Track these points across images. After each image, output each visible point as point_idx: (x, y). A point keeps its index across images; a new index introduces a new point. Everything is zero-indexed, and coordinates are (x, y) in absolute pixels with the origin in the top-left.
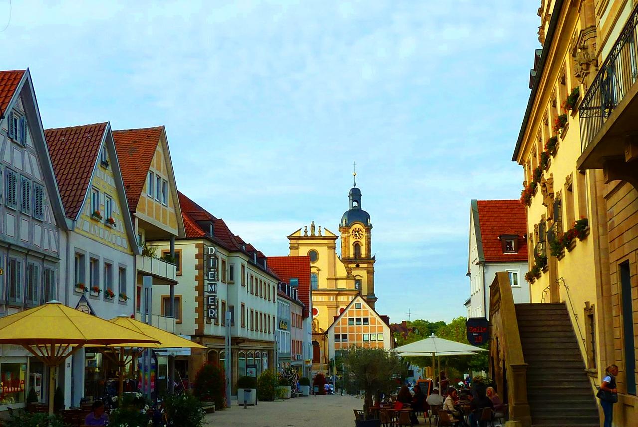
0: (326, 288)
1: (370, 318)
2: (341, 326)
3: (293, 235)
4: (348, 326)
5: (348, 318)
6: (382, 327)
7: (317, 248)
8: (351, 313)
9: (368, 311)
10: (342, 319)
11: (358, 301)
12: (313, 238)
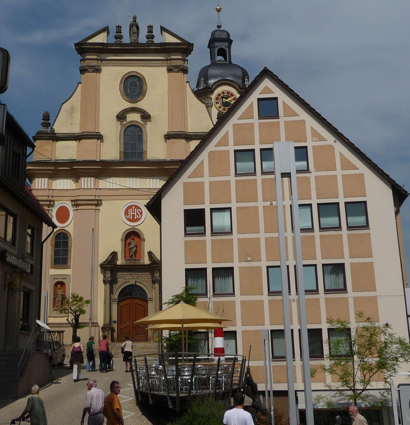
0: (166, 158)
1: (314, 147)
2: (206, 179)
3: (90, 41)
4: (232, 178)
5: (231, 148)
6: (362, 175)
7: (144, 71)
8: (243, 132)
9: (304, 121)
10: (211, 154)
11: (267, 90)
12: (135, 48)
